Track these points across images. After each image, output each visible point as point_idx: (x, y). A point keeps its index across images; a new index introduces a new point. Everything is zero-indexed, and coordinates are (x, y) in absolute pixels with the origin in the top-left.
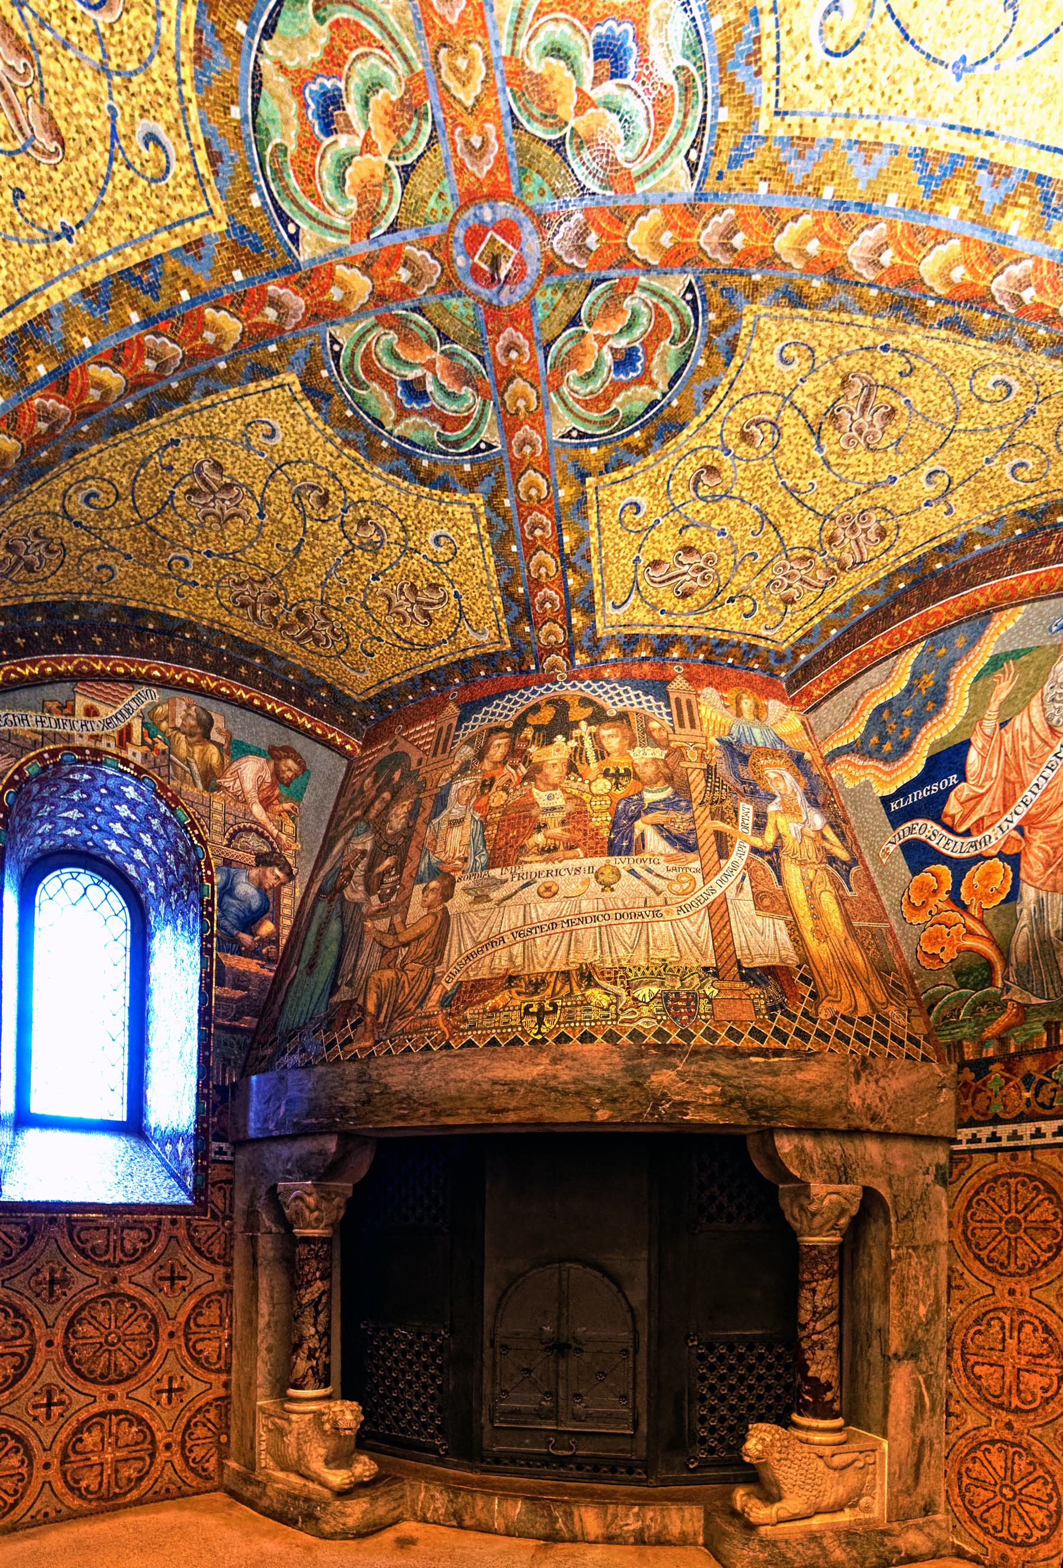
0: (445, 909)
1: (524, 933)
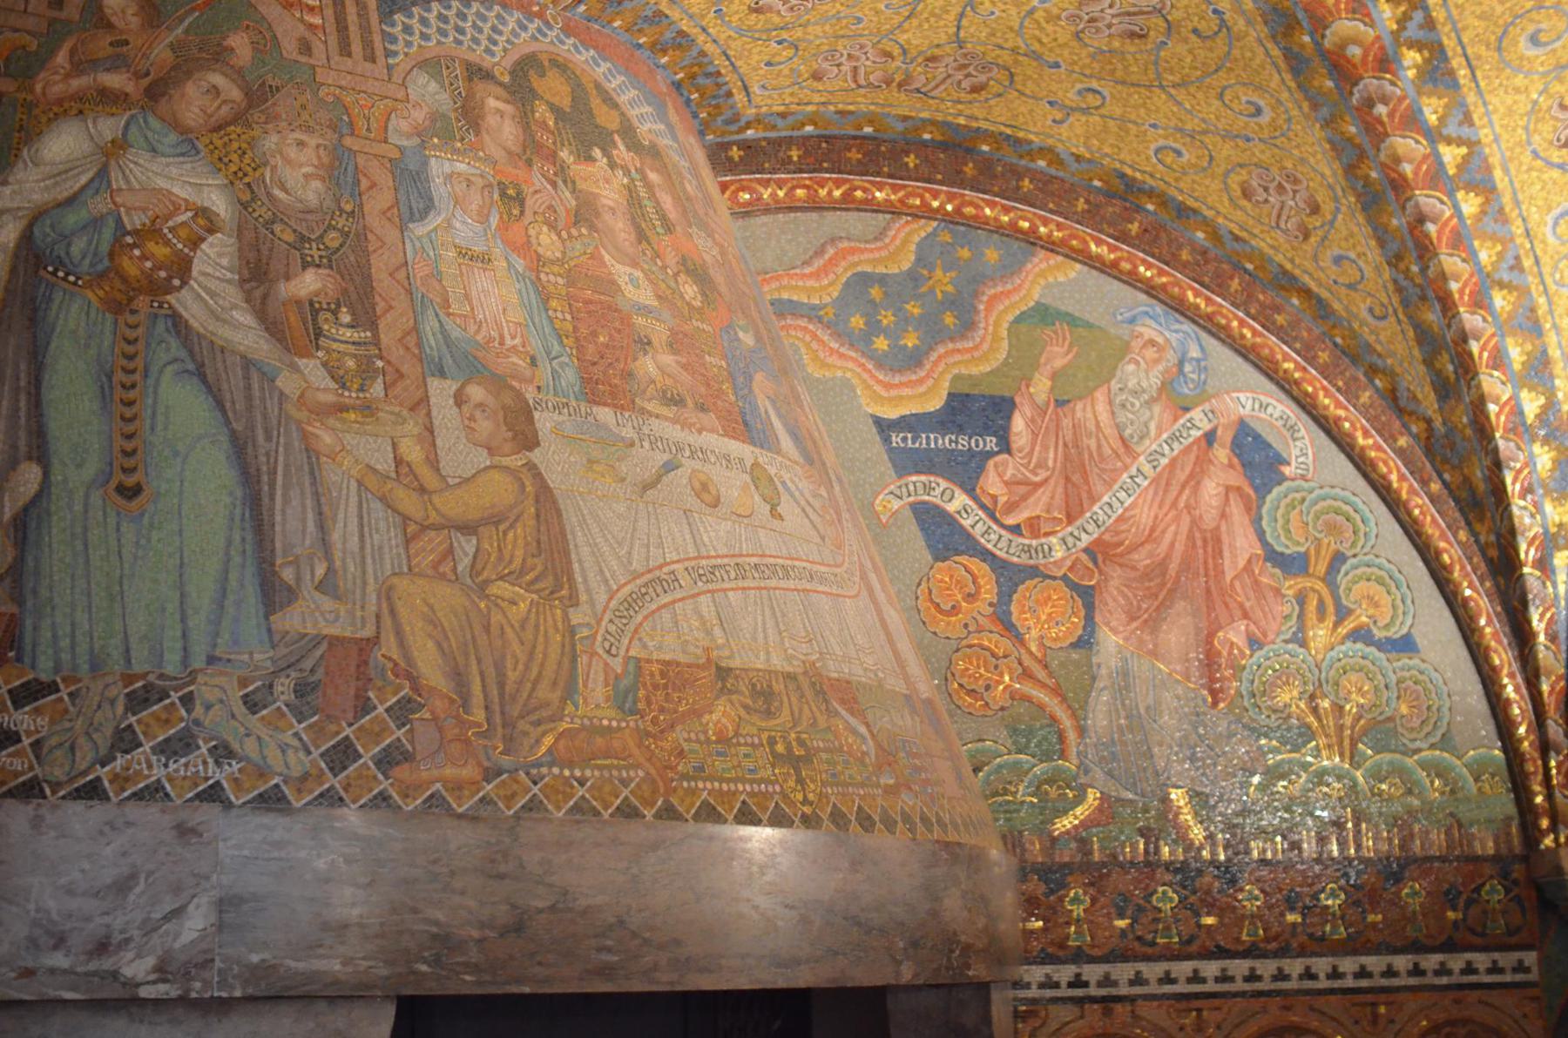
0: (531, 467)
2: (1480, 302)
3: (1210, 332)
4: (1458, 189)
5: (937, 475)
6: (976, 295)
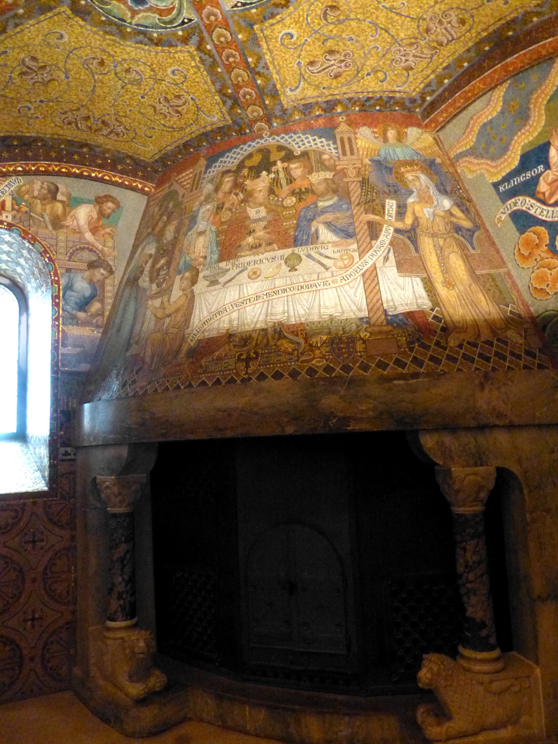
1: (240, 304)
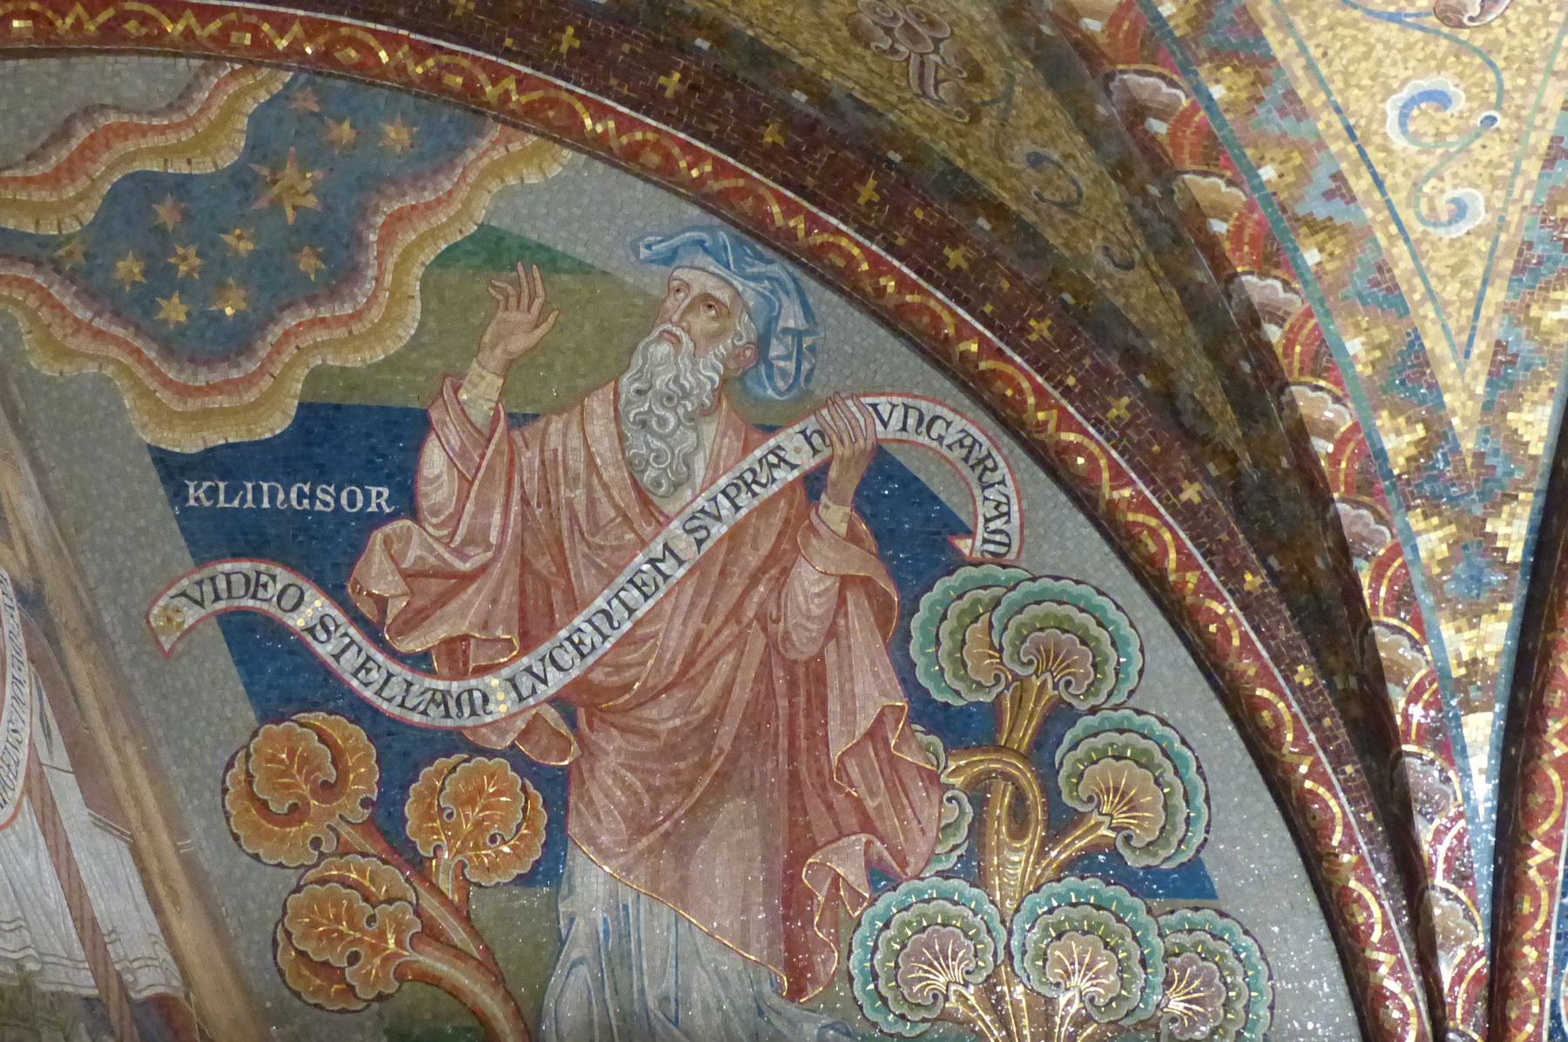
2: (1273, 258)
3: (822, 279)
4: (1200, 62)
5: (273, 559)
6: (363, 212)
